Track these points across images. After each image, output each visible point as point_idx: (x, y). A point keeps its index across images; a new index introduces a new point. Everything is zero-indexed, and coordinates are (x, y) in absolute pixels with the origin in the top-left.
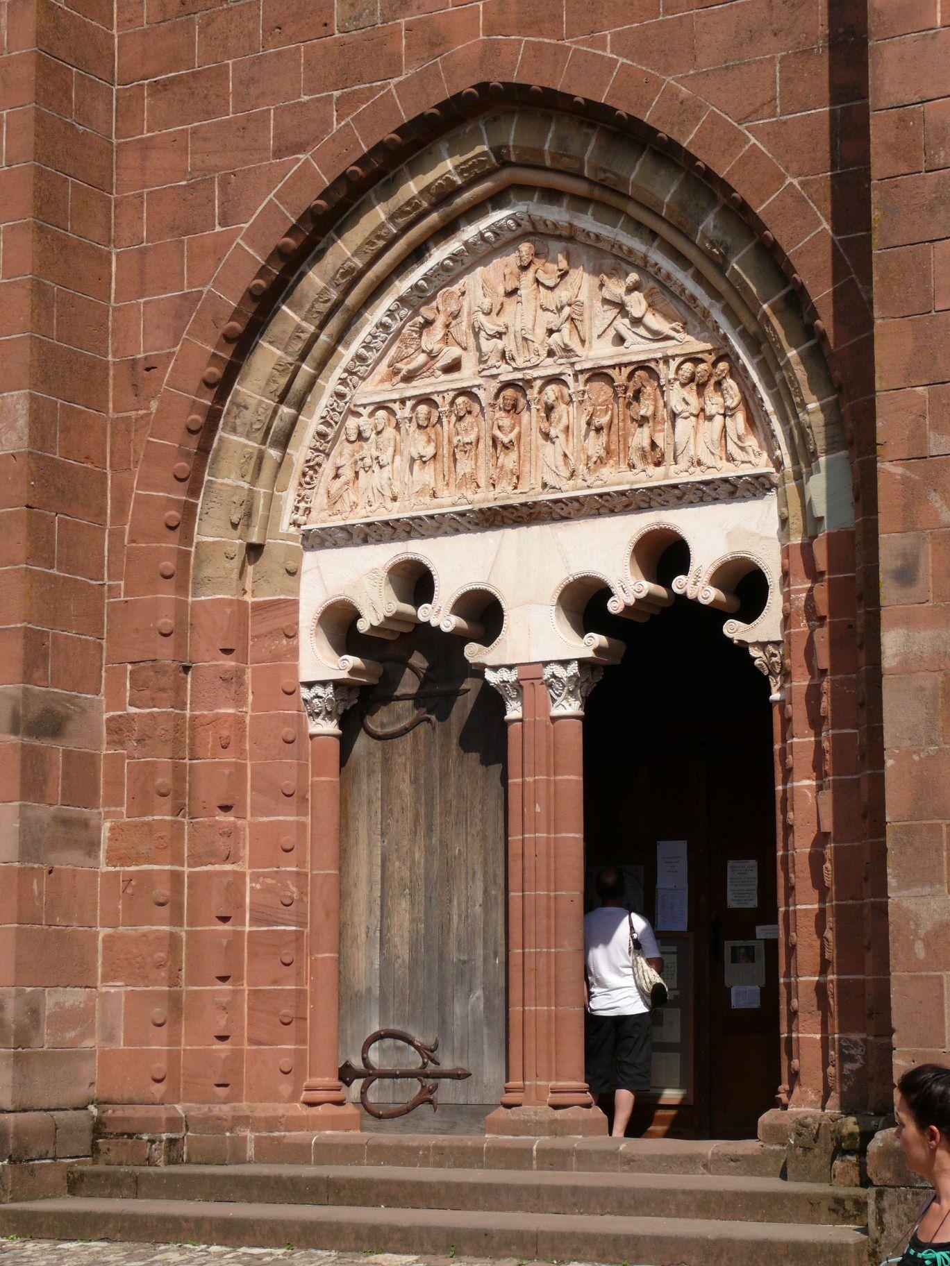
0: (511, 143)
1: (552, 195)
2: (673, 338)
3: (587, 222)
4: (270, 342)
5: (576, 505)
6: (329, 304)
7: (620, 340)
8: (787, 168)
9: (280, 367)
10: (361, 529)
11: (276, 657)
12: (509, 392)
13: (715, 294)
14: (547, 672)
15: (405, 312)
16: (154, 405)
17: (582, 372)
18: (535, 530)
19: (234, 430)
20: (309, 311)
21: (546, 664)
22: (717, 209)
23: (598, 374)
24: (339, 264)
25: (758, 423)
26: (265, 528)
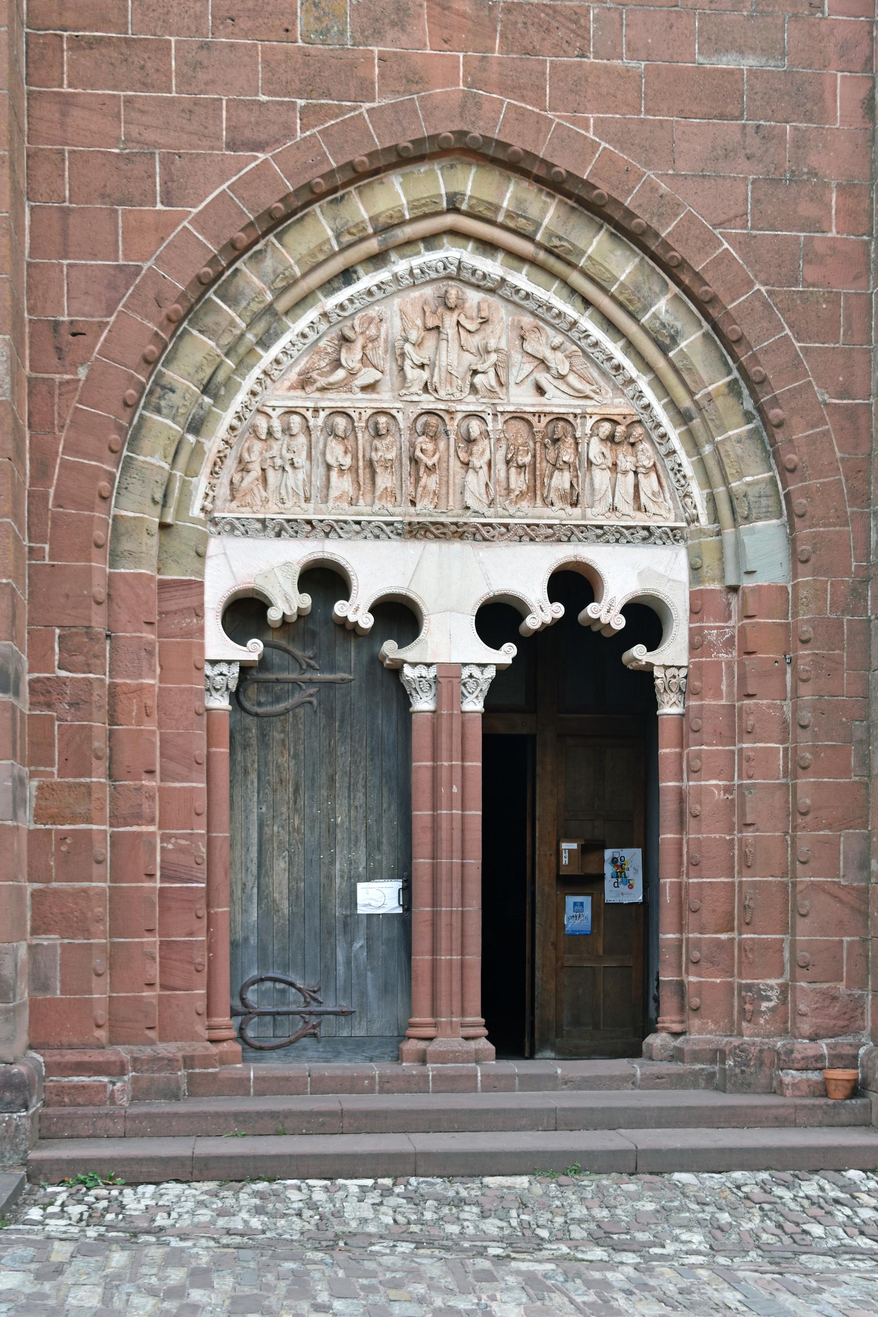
0: (468, 193)
1: (488, 246)
2: (592, 399)
3: (521, 279)
4: (200, 331)
5: (503, 530)
6: (262, 306)
7: (540, 390)
8: (756, 276)
9: (208, 357)
10: (281, 524)
11: (189, 634)
12: (433, 420)
13: (647, 367)
14: (466, 672)
15: (323, 327)
16: (82, 373)
17: (502, 413)
18: (457, 547)
19: (158, 411)
20: (245, 308)
21: (465, 665)
22: (669, 296)
23: (518, 417)
24: (281, 269)
25: (664, 484)
26: (177, 512)
